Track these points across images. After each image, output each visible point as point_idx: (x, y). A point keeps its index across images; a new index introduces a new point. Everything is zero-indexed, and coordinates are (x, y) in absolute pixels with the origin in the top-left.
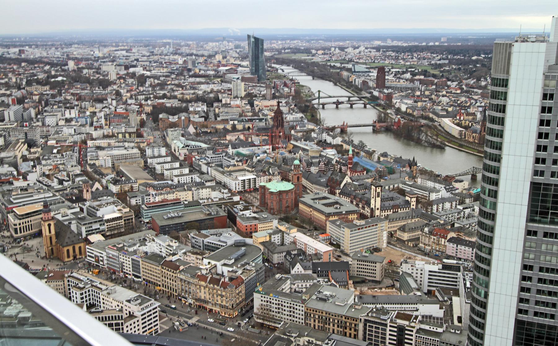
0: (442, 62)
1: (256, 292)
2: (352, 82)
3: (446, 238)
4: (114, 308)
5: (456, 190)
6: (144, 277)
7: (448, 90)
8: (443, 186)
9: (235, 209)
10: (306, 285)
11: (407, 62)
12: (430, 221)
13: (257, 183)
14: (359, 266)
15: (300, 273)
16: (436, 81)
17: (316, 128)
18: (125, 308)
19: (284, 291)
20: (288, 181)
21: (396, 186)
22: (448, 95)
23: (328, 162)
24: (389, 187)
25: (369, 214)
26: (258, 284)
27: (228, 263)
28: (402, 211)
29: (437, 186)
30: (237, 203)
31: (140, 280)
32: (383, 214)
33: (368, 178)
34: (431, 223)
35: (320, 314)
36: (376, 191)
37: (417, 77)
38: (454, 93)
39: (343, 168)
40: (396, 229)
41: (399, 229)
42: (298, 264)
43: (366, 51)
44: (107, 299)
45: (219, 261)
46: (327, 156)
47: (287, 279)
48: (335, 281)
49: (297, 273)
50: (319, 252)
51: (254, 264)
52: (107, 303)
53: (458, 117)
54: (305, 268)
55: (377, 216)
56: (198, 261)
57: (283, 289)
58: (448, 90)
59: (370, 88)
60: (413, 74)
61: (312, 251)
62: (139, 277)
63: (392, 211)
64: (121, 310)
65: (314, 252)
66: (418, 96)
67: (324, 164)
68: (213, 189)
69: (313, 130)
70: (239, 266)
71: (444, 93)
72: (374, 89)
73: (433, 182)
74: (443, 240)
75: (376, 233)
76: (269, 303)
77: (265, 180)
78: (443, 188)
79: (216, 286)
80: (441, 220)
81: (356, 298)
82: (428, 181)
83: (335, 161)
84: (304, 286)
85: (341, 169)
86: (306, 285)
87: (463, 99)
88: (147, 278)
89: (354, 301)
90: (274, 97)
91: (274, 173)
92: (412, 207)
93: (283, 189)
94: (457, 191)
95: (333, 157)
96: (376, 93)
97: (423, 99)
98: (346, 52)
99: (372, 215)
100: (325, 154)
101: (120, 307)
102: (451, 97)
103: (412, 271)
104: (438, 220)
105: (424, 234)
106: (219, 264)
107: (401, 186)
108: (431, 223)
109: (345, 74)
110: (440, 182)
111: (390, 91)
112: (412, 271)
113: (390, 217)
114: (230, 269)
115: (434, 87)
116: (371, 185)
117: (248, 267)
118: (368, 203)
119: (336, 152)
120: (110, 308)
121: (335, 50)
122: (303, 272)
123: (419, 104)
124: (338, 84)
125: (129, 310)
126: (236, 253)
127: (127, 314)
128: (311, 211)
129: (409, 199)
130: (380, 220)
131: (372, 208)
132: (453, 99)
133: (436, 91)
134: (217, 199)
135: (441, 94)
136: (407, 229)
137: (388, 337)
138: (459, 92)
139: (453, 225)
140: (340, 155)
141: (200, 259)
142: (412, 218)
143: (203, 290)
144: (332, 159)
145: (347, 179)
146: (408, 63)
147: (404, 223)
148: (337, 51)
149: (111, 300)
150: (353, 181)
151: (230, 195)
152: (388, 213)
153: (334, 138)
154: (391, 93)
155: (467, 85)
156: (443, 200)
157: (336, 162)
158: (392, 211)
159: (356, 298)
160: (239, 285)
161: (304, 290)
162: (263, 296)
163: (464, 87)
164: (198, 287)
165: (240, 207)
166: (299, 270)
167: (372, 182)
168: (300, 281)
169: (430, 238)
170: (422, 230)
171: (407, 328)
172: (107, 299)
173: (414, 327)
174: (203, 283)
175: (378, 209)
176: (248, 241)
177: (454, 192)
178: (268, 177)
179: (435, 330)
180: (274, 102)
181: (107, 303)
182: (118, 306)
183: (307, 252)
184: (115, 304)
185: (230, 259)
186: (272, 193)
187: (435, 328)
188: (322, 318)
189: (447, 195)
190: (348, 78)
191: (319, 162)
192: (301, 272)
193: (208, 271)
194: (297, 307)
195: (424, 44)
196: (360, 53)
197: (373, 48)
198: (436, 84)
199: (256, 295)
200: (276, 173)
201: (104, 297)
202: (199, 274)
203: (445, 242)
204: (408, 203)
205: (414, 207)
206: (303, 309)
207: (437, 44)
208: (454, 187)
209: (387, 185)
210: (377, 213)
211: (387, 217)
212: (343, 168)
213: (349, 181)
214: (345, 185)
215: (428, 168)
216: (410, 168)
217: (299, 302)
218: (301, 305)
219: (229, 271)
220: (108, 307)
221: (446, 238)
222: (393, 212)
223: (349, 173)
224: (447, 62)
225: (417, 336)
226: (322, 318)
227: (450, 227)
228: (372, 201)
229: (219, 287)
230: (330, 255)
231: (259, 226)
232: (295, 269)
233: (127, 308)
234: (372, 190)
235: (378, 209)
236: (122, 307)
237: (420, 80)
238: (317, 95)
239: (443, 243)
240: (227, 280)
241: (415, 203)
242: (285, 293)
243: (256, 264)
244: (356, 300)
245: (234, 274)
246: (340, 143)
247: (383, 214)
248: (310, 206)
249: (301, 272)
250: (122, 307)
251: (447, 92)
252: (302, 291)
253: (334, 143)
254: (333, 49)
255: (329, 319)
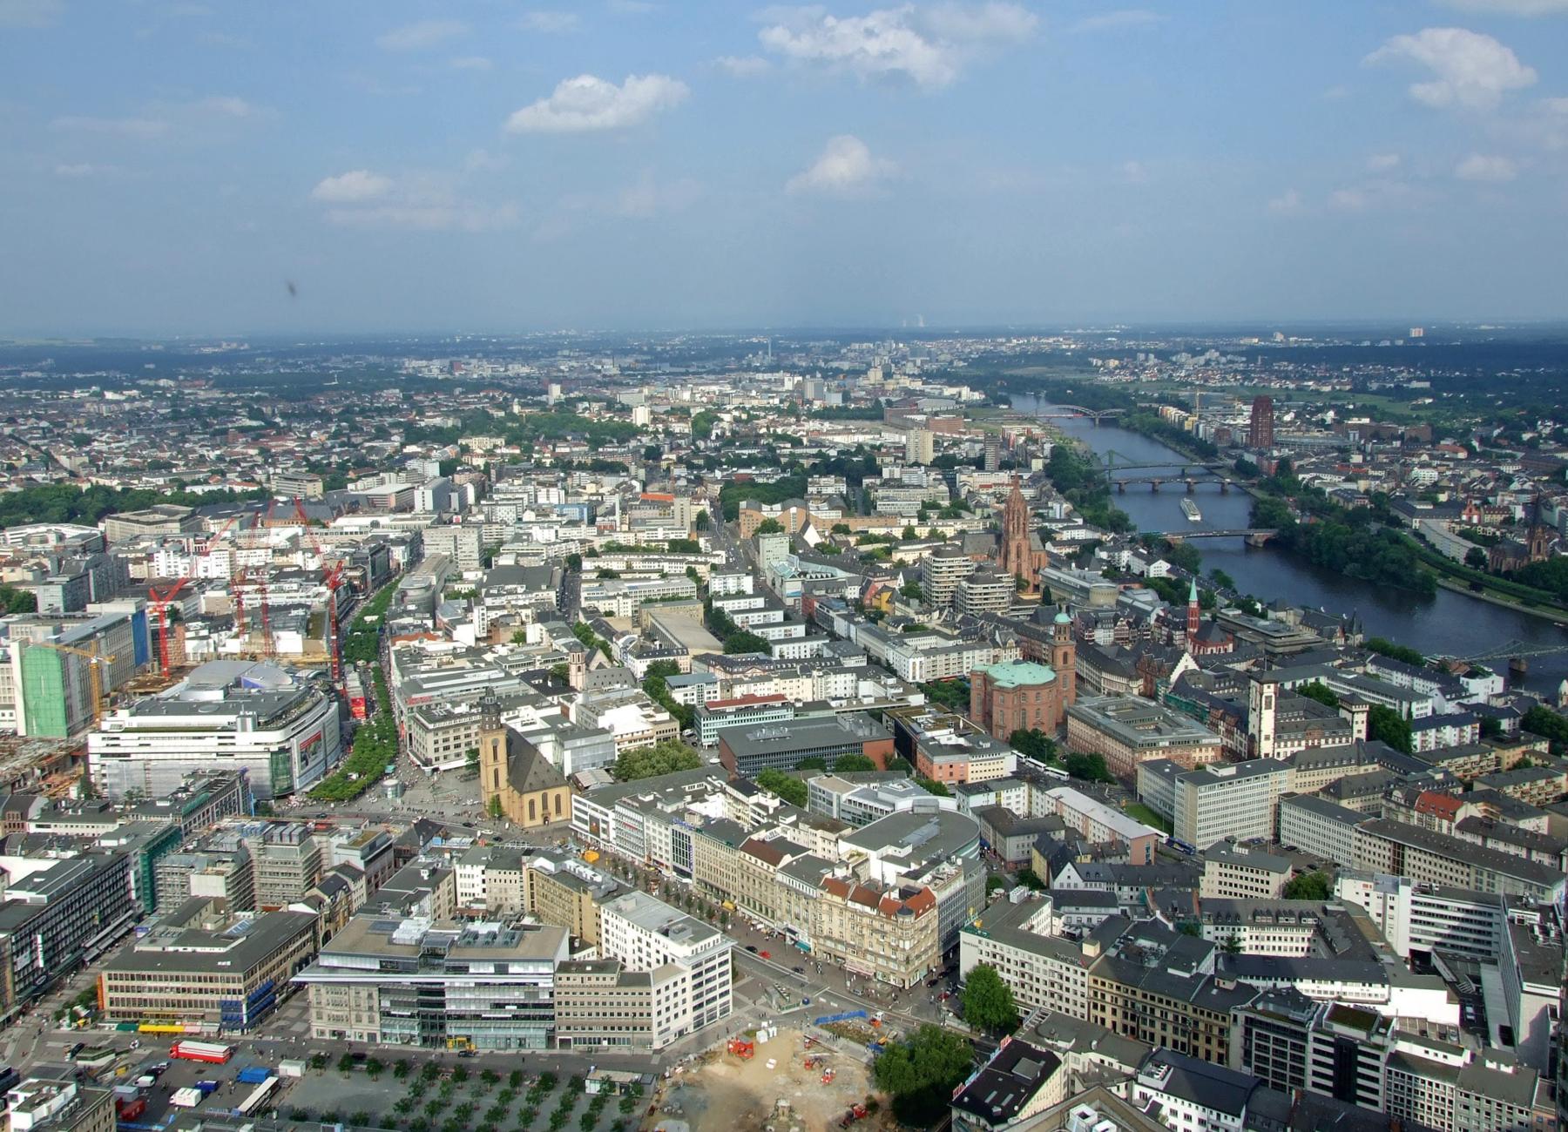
0: (1415, 385)
1: (966, 930)
2: (1189, 432)
3: (1452, 820)
5: (1471, 696)
7: (1435, 452)
8: (1435, 686)
9: (914, 726)
10: (1089, 920)
11: (1324, 384)
12: (1406, 773)
13: (965, 666)
14: (1224, 879)
15: (1072, 888)
16: (1401, 429)
17: (1104, 538)
19: (1035, 931)
20: (1040, 661)
21: (1312, 680)
22: (1435, 463)
23: (1139, 617)
24: (1294, 684)
25: (1244, 750)
26: (971, 910)
27: (897, 854)
28: (1330, 745)
29: (1420, 685)
30: (919, 710)
32: (1281, 751)
33: (1239, 661)
34: (1408, 778)
35: (1129, 995)
36: (1261, 695)
37: (1355, 421)
38: (1448, 460)
39: (1178, 636)
40: (1316, 788)
41: (1325, 790)
42: (1069, 865)
43: (1223, 360)
45: (875, 848)
46: (1136, 604)
47: (1042, 902)
48: (1162, 913)
49: (1065, 888)
50: (1120, 838)
51: (959, 862)
53: (1464, 518)
54: (1086, 876)
55: (1267, 755)
56: (826, 845)
57: (1032, 927)
58: (1435, 452)
59: (1234, 446)
60: (1343, 414)
61: (1101, 835)
63: (1303, 743)
65: (1107, 839)
66: (1357, 465)
67: (1128, 623)
68: (861, 674)
69: (1099, 543)
70: (924, 863)
71: (1425, 457)
72: (1246, 448)
73: (1409, 674)
74: (1445, 823)
75: (1265, 797)
76: (998, 960)
77: (985, 658)
78: (1437, 692)
79: (867, 909)
80: (1437, 773)
81: (1221, 960)
82: (1394, 673)
83: (1154, 616)
84: (1085, 921)
85: (1170, 638)
86: (1089, 920)
87: (1476, 473)
89: (1216, 970)
90: (1004, 466)
91: (1005, 644)
92: (1356, 735)
93: (1029, 681)
94: (1473, 701)
95: (1149, 608)
96: (1250, 458)
97: (1371, 472)
98: (1175, 363)
99: (1252, 755)
100: (1130, 601)
102: (1442, 469)
103: (1367, 899)
104: (1429, 772)
105: (1393, 806)
106: (873, 855)
107: (1323, 681)
108: (1408, 778)
109: (1172, 413)
110: (1427, 677)
111: (1286, 452)
112: (1367, 899)
113: (1298, 760)
114: (904, 870)
115: (1397, 444)
116: (1251, 677)
117: (946, 867)
118: (1242, 724)
119: (1156, 597)
121: (1147, 360)
122: (1081, 886)
123: (1362, 485)
124: (1155, 436)
126: (917, 832)
128: (1098, 737)
129: (1348, 716)
130: (1272, 765)
131: (1253, 736)
132: (1449, 473)
133: (1404, 455)
134: (871, 700)
135: (1416, 460)
136: (1345, 789)
137: (1310, 1068)
138: (1462, 455)
139: (1468, 787)
140: (1166, 603)
141: (830, 841)
142: (1359, 764)
143: (836, 918)
144: (1148, 614)
145: (1187, 663)
146: (1327, 389)
147: (1337, 776)
148: (1152, 359)
150: (1201, 667)
151: (901, 690)
152: (1296, 749)
153: (1149, 563)
154: (1289, 457)
155: (1482, 441)
156: (1437, 721)
157: (1157, 620)
158: (1303, 743)
159: (1221, 960)
160: (925, 911)
161: (1086, 932)
162: (984, 940)
163: (1475, 443)
164: (825, 907)
165: (921, 719)
166: (1072, 882)
167: (1248, 671)
168: (1073, 909)
169: (1409, 817)
170: (1388, 795)
171: (1360, 1048)
173: (1381, 1048)
174: (838, 899)
175: (1267, 738)
176: (948, 804)
177: (1465, 701)
178: (993, 652)
179: (1440, 1059)
180: (1004, 477)
183: (1090, 836)
185: (902, 846)
186: (1002, 689)
187: (1441, 1054)
188: (1133, 1005)
189: (1451, 708)
190: (1181, 423)
191: (1116, 620)
192: (1076, 885)
193: (850, 871)
194: (1071, 975)
195: (1367, 343)
196: (1207, 363)
197: (1241, 354)
198: (1401, 437)
199: (964, 937)
200: (1011, 641)
202: (829, 876)
203: (1449, 829)
204: (1347, 725)
205: (1363, 736)
206: (1085, 979)
207: (1400, 342)
208: (1466, 690)
209: (1288, 680)
210: (1266, 747)
211: (1291, 761)
212: (1178, 636)
213: (1193, 666)
214: (1182, 676)
215: (1393, 642)
216: (1346, 640)
217: (1072, 963)
218: (1080, 970)
219: (899, 874)
221: (1452, 820)
222: (1307, 746)
223: (1190, 648)
224: (1427, 385)
225: (1390, 1072)
226: (1133, 1005)
227: (1460, 790)
228: (1252, 718)
229: (875, 913)
230: (1148, 849)
231: (970, 769)
232: (1062, 877)
234: (1253, 690)
235: (1267, 738)
237: (1361, 427)
238: (1105, 461)
239: (1445, 831)
240: (895, 895)
241: (1363, 727)
242: (1038, 937)
243: (965, 859)
244: (1221, 966)
245: (911, 882)
246: (1164, 574)
247: (1281, 751)
248: (1095, 726)
249: (1076, 885)
251: (1432, 457)
252: (1081, 935)
253: (1152, 575)
254: (1142, 356)
255: (1152, 1011)
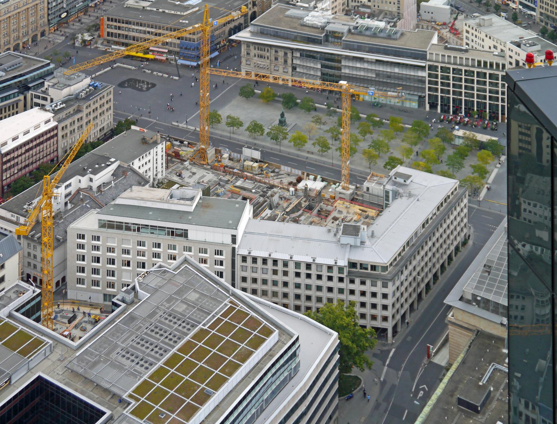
4: (486, 48)
6: (543, 11)
18: (508, 53)
31: (533, 13)
44: (475, 33)
52: (475, 39)
62: (533, 10)
64: (502, 55)
88: (549, 13)
101: (499, 50)
120: (481, 49)
125: (515, 57)
127: (511, 63)
149: (483, 36)
172: (475, 33)
181: (475, 39)
182: (495, 47)
184: (488, 43)
201: (469, 29)
220: (475, 46)
233: (512, 54)
236: (502, 51)
250: (502, 51)
